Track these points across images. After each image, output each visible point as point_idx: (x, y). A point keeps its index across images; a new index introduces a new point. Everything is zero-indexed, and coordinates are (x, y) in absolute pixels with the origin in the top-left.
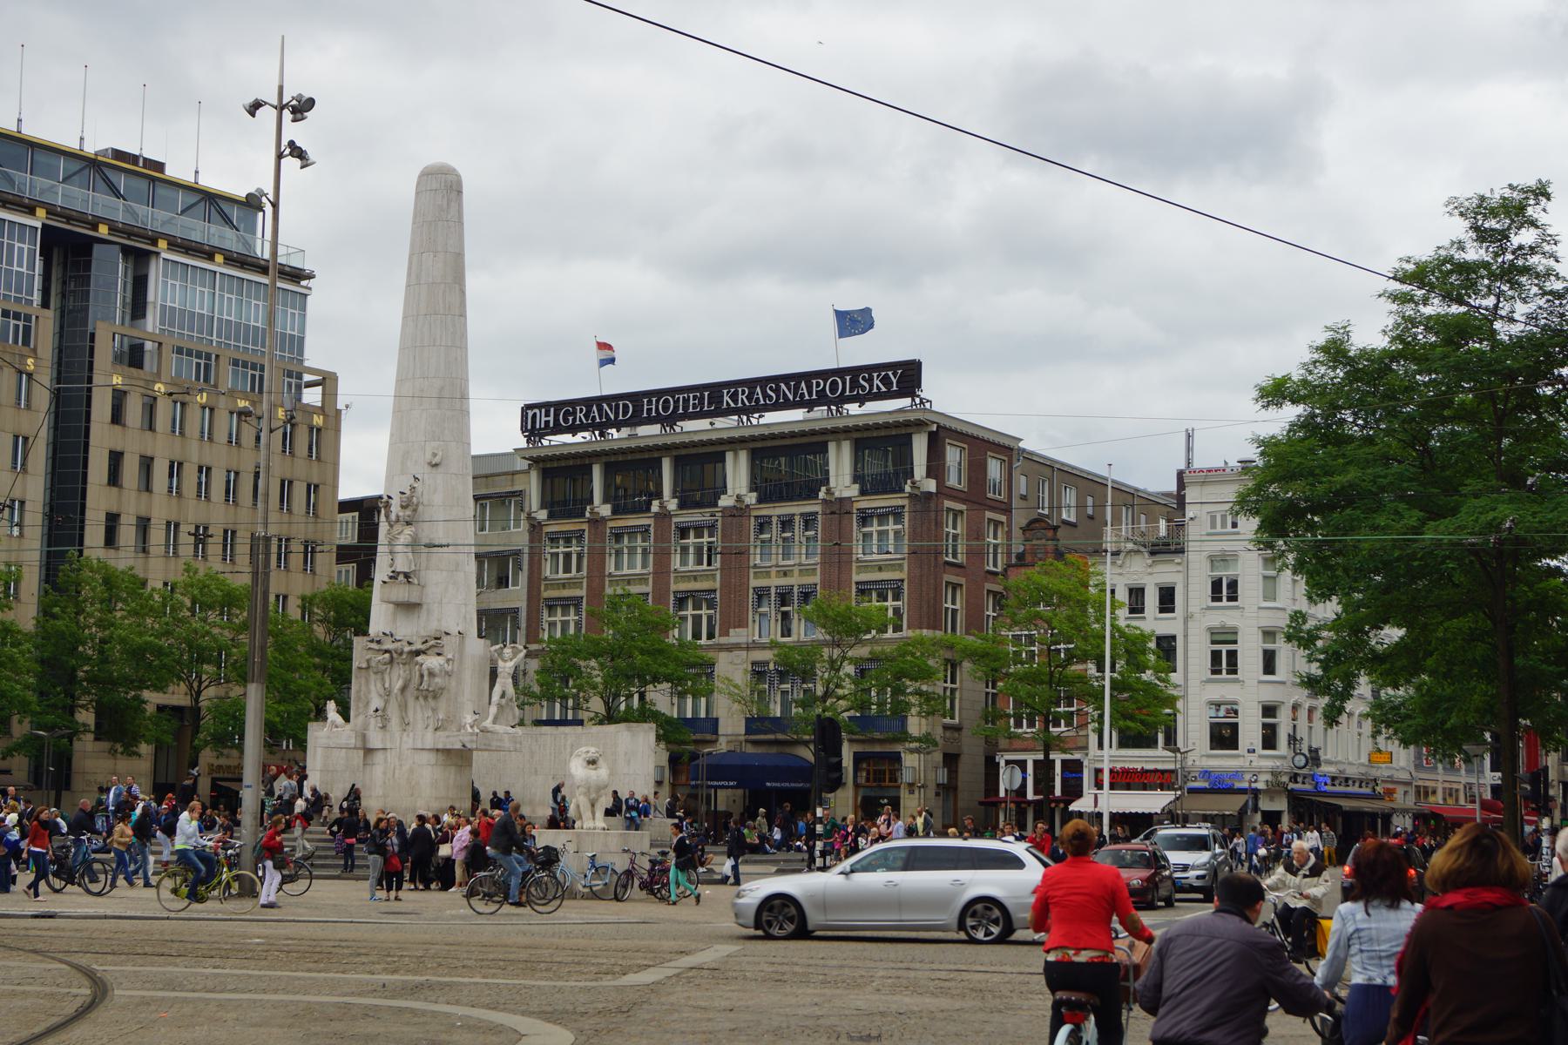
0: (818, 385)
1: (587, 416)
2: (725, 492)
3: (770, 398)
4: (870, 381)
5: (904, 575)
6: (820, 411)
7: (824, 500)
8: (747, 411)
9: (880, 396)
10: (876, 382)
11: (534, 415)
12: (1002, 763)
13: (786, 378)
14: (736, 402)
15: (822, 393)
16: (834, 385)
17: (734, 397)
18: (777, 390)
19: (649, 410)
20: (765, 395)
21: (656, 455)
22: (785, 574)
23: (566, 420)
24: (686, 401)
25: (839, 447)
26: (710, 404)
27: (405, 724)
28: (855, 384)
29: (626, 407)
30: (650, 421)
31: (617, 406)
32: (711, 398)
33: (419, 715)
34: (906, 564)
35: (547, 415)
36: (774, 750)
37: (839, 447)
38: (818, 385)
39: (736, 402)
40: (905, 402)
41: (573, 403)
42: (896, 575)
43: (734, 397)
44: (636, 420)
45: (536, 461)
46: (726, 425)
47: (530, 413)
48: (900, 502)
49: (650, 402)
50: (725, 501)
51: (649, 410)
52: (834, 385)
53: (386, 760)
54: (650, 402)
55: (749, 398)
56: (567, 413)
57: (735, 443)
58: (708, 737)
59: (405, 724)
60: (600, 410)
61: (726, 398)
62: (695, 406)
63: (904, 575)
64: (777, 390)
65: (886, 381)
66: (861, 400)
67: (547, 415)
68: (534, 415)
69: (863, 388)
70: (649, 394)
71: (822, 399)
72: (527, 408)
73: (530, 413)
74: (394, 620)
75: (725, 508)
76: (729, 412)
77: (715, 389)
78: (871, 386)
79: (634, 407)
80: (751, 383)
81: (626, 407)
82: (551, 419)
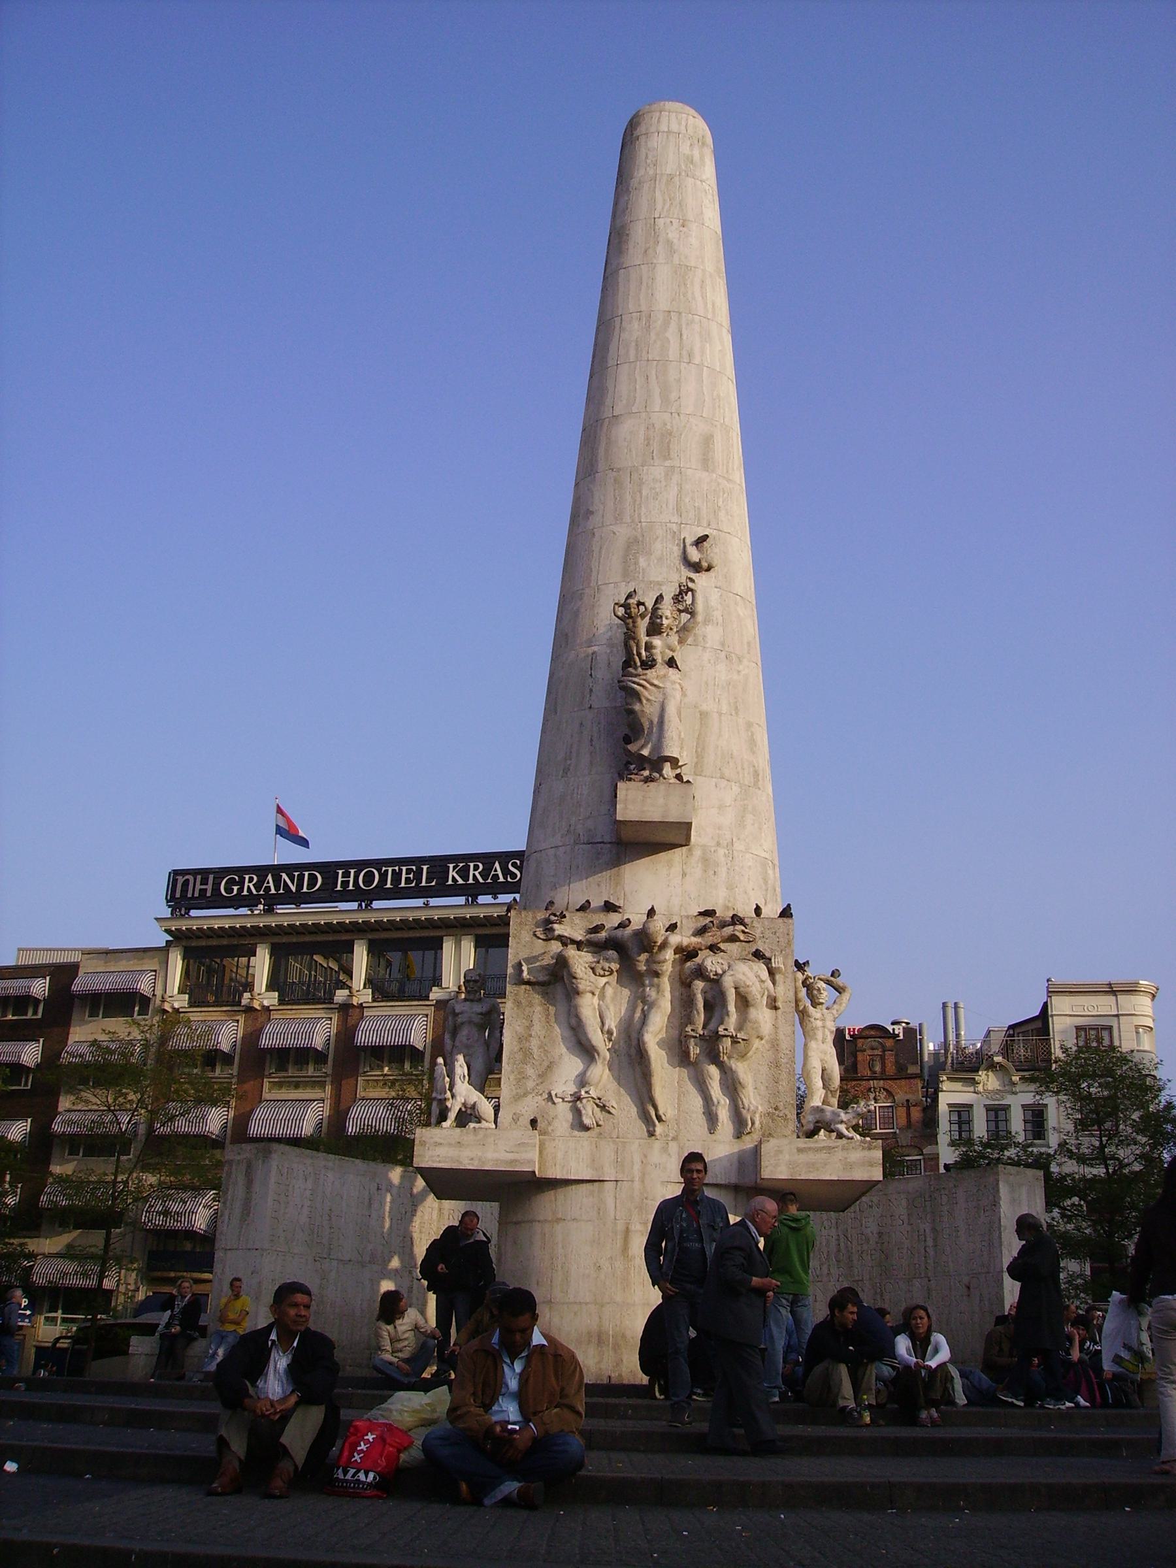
1: (258, 886)
2: (439, 985)
3: (514, 876)
8: (472, 892)
11: (186, 882)
14: (466, 878)
17: (464, 873)
19: (345, 884)
20: (506, 872)
21: (345, 937)
23: (229, 890)
24: (397, 876)
26: (429, 880)
29: (313, 880)
30: (345, 896)
31: (301, 877)
32: (434, 873)
35: (204, 882)
39: (465, 877)
41: (242, 871)
43: (464, 873)
44: (329, 894)
45: (178, 937)
46: (450, 906)
47: (181, 880)
49: (346, 875)
50: (436, 994)
51: (345, 884)
54: (346, 875)
56: (231, 882)
57: (458, 927)
60: (277, 881)
61: (452, 873)
62: (408, 880)
67: (204, 882)
68: (186, 882)
70: (346, 865)
72: (176, 873)
73: (181, 880)
76: (455, 891)
77: (438, 864)
79: (329, 879)
80: (488, 859)
81: (313, 880)
82: (209, 887)
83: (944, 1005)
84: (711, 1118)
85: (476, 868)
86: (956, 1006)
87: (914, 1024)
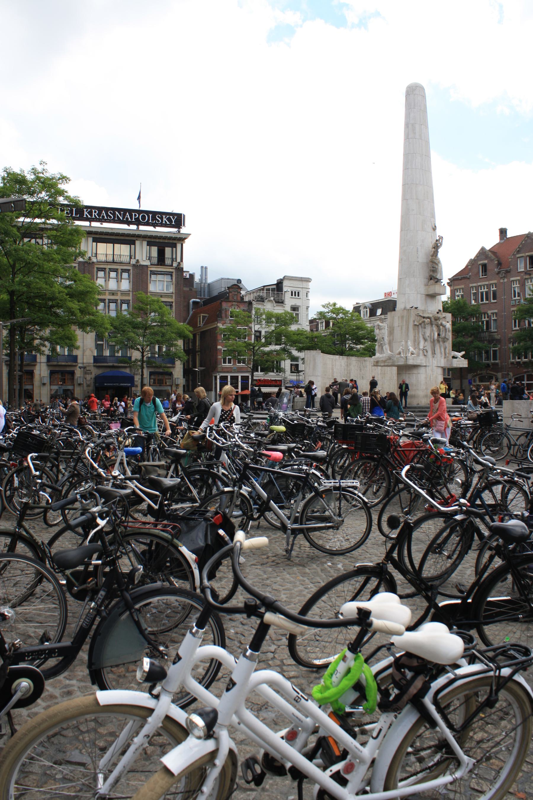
0: (135, 215)
3: (110, 217)
4: (162, 218)
5: (173, 300)
6: (133, 227)
7: (134, 265)
8: (90, 220)
9: (166, 226)
10: (164, 219)
12: (218, 377)
13: (119, 210)
14: (91, 215)
15: (137, 220)
16: (143, 218)
17: (90, 213)
18: (114, 214)
20: (107, 215)
22: (113, 294)
25: (142, 245)
27: (434, 353)
28: (154, 218)
33: (439, 350)
34: (174, 295)
36: (108, 370)
37: (142, 245)
38: (135, 215)
40: (174, 230)
42: (169, 300)
43: (90, 213)
48: (171, 270)
52: (143, 218)
53: (426, 371)
55: (99, 215)
58: (74, 364)
59: (434, 353)
61: (85, 213)
63: (173, 300)
64: (114, 214)
65: (169, 220)
66: (155, 226)
69: (158, 221)
71: (138, 223)
74: (426, 303)
75: (80, 262)
76: (87, 219)
78: (162, 220)
83: (202, 267)
84: (441, 353)
85: (95, 212)
86: (206, 268)
87: (191, 272)
